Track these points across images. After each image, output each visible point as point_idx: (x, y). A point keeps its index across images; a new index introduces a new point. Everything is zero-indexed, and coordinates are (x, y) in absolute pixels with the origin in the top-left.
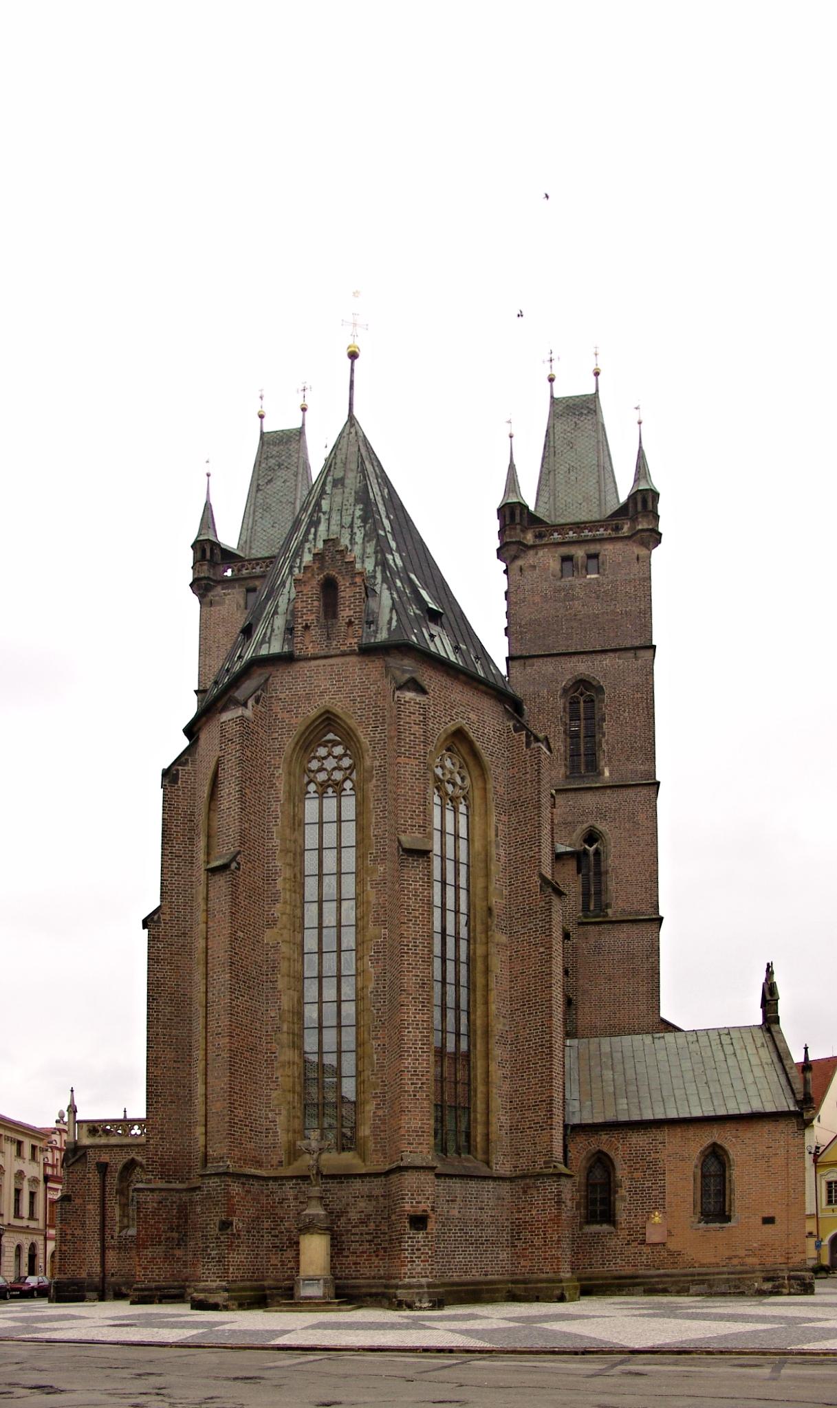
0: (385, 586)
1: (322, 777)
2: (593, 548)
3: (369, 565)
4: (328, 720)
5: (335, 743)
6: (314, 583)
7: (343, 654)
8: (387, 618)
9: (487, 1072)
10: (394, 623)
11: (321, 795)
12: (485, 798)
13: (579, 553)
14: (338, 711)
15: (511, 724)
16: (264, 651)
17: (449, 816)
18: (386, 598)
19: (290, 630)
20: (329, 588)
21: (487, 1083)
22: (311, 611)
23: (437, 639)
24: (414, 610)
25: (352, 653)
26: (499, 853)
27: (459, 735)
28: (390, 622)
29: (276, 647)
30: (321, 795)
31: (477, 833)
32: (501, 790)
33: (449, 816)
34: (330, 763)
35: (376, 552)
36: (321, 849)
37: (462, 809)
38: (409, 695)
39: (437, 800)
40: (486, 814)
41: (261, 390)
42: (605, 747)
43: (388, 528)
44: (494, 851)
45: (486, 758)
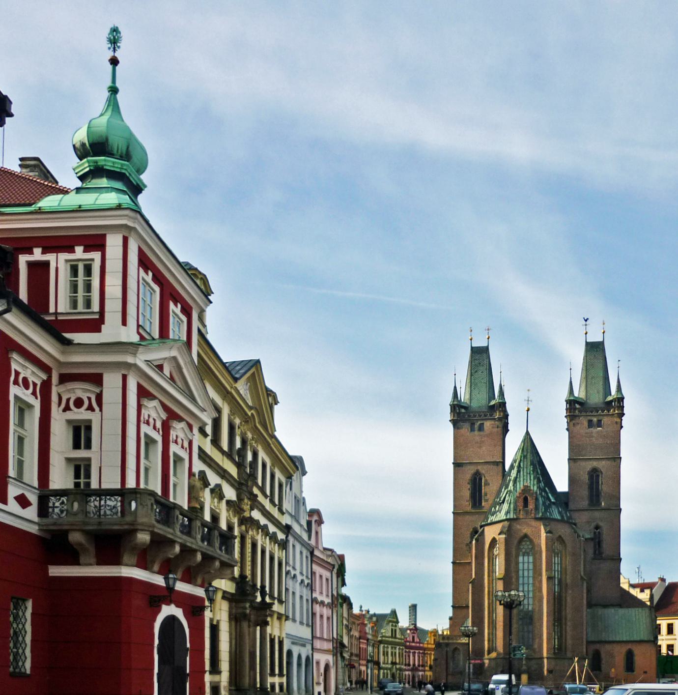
0: (540, 496)
1: (524, 550)
2: (600, 418)
3: (535, 488)
4: (526, 536)
5: (528, 541)
6: (522, 498)
7: (531, 518)
8: (541, 508)
9: (566, 629)
10: (543, 510)
11: (524, 556)
12: (566, 552)
13: (595, 420)
14: (529, 534)
15: (573, 531)
16: (508, 517)
17: (556, 558)
18: (541, 500)
19: (515, 509)
20: (526, 500)
21: (566, 632)
22: (521, 504)
23: (554, 512)
24: (548, 503)
25: (532, 518)
26: (569, 568)
27: (560, 537)
28: (542, 509)
29: (512, 515)
30: (524, 556)
31: (563, 562)
32: (570, 550)
33: (556, 558)
34: (526, 547)
35: (537, 484)
36: (523, 570)
37: (559, 555)
38: (549, 535)
39: (553, 555)
40: (566, 557)
41: (471, 328)
42: (603, 494)
43: (539, 473)
44: (568, 567)
45: (566, 542)
